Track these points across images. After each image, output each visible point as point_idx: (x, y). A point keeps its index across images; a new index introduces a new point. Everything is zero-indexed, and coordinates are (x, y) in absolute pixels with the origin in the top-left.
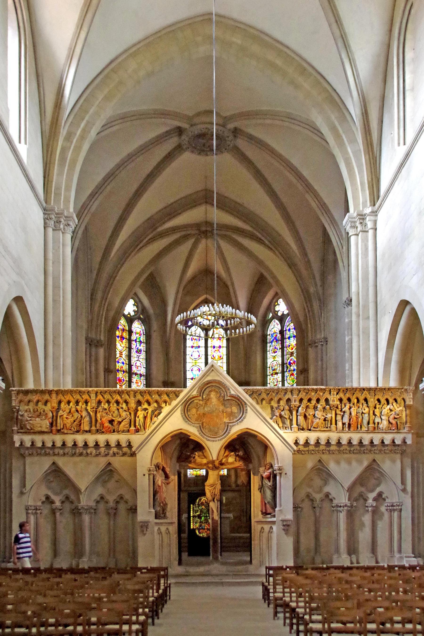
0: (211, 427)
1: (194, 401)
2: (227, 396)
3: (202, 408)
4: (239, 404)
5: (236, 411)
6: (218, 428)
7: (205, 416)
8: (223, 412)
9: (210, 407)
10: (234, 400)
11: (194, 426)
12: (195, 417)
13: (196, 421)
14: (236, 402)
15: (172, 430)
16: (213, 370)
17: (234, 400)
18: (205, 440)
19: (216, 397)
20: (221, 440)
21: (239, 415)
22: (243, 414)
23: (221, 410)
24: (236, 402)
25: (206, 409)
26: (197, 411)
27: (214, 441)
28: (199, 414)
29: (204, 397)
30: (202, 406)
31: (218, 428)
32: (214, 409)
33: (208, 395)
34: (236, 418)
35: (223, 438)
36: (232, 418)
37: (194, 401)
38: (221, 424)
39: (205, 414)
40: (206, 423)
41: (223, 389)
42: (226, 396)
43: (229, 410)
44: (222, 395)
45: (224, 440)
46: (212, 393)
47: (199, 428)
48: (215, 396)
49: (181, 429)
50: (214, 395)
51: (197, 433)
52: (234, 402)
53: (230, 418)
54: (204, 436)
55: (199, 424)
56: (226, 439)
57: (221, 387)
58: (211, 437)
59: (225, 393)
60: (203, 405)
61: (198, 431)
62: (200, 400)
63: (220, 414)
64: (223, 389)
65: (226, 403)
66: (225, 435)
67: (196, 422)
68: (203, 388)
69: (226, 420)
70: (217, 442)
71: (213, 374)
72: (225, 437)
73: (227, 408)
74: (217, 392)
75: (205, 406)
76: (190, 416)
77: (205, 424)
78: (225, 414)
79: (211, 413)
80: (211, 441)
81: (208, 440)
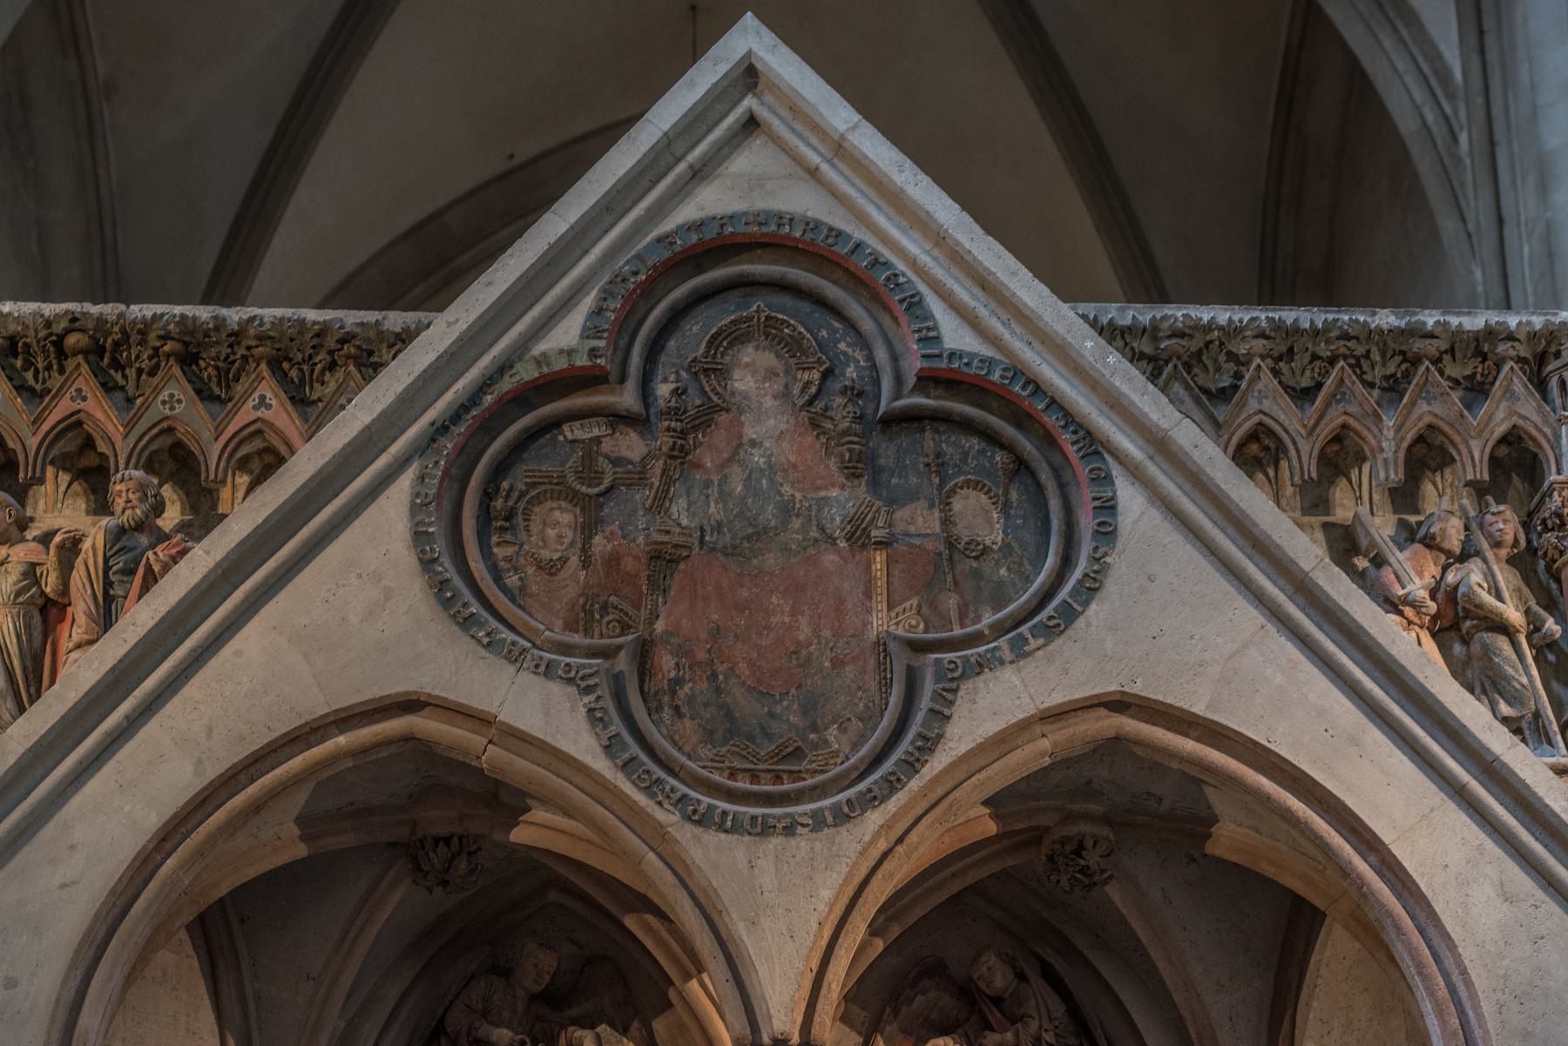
0: (737, 695)
1: (555, 424)
2: (899, 380)
3: (642, 496)
4: (1021, 467)
5: (994, 536)
6: (808, 708)
7: (675, 584)
8: (858, 536)
9: (724, 496)
10: (967, 426)
11: (549, 671)
12: (571, 592)
13: (571, 627)
14: (993, 439)
15: (317, 705)
16: (751, 123)
17: (967, 426)
18: (666, 817)
19: (785, 394)
20: (842, 817)
21: (1028, 580)
22: (1067, 562)
23: (835, 518)
24: (993, 439)
25: (679, 508)
26: (588, 528)
27: (764, 829)
28: (613, 560)
29: (663, 390)
30: (638, 477)
31: (809, 707)
32: (770, 515)
33: (712, 369)
34: (999, 603)
35: (871, 800)
36: (951, 602)
37: (555, 424)
38: (837, 663)
39: (674, 561)
40: (681, 652)
41: (856, 310)
42: (887, 384)
43: (920, 520)
44: (851, 372)
45: (875, 818)
46: (748, 354)
47: (604, 691)
48: (777, 385)
49: (410, 704)
50: (771, 374)
51: (582, 744)
52: (974, 443)
53: (933, 605)
54: (659, 773)
55: (607, 653)
56: (894, 804)
57: (832, 291)
58: (732, 796)
59: (882, 355)
60: (659, 465)
61: (595, 718)
62: (619, 419)
63: (829, 559)
64: (856, 310)
65: (887, 451)
66: (888, 765)
67: (576, 638)
68: (648, 292)
69: (907, 623)
70: (802, 844)
71: (749, 159)
72: (892, 785)
73: (893, 502)
74: (792, 347)
75: (667, 480)
76: (512, 580)
77: (666, 663)
78: (879, 558)
79: (731, 552)
80: (736, 828)
81: (702, 819)
